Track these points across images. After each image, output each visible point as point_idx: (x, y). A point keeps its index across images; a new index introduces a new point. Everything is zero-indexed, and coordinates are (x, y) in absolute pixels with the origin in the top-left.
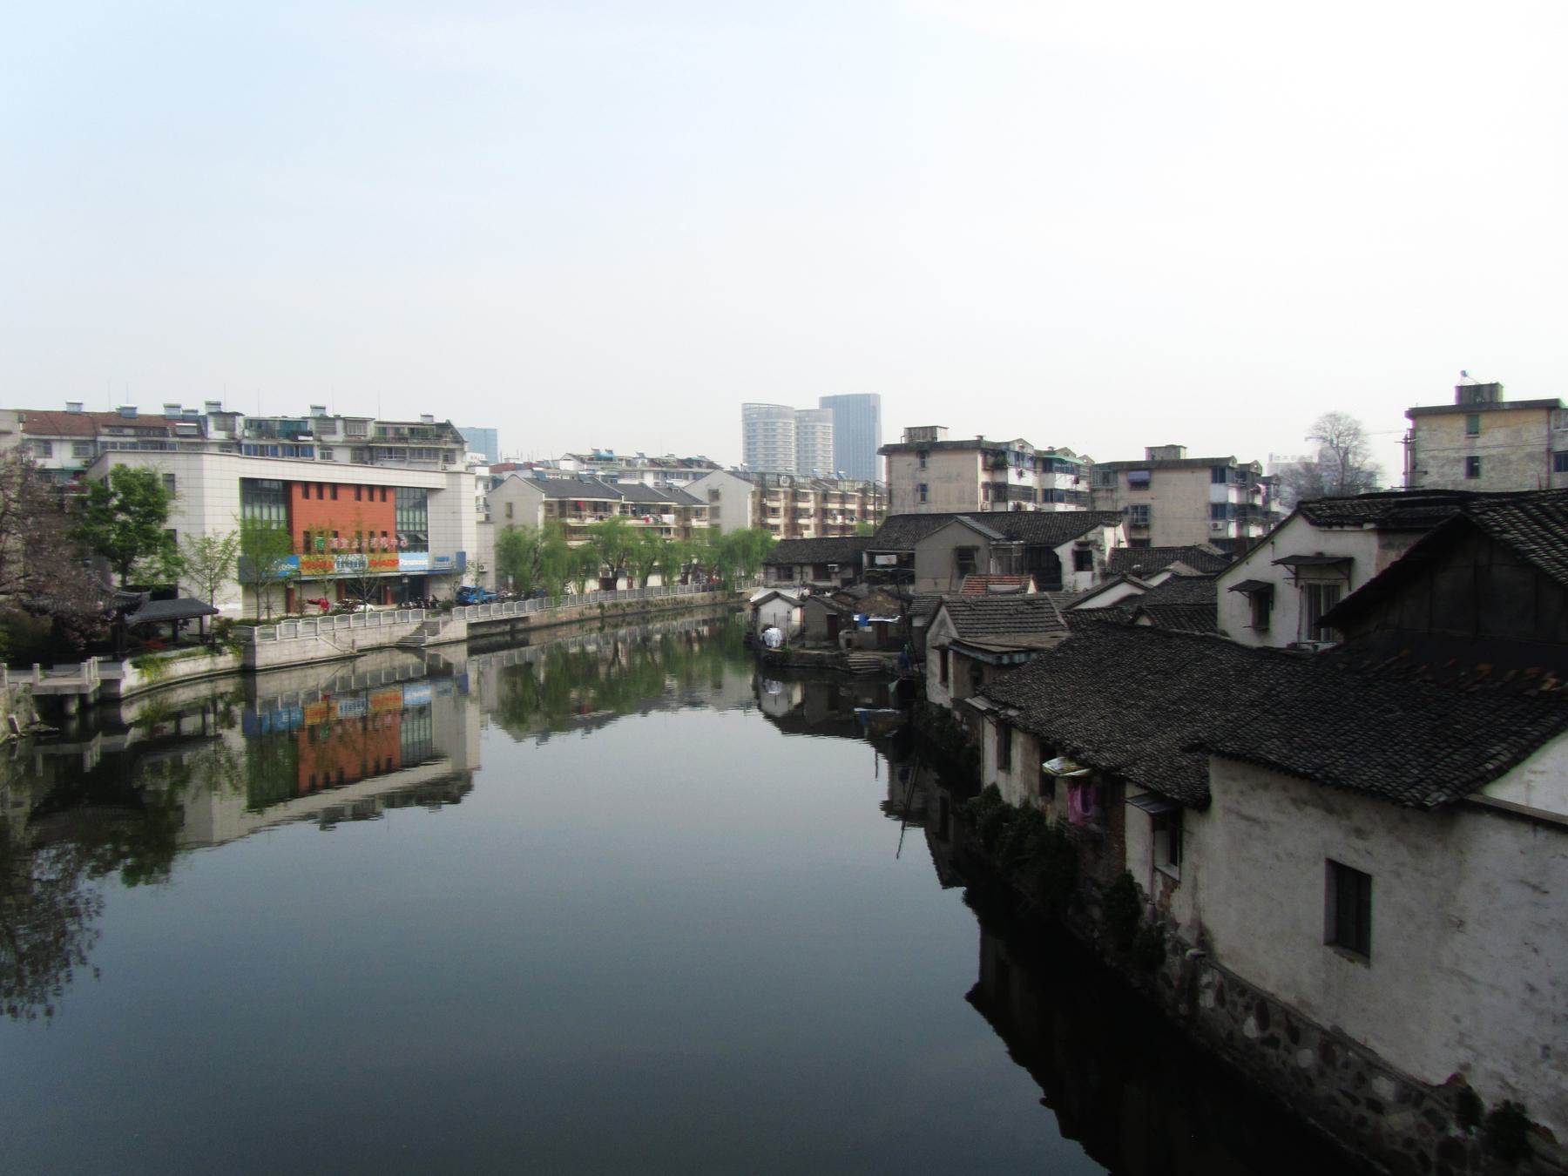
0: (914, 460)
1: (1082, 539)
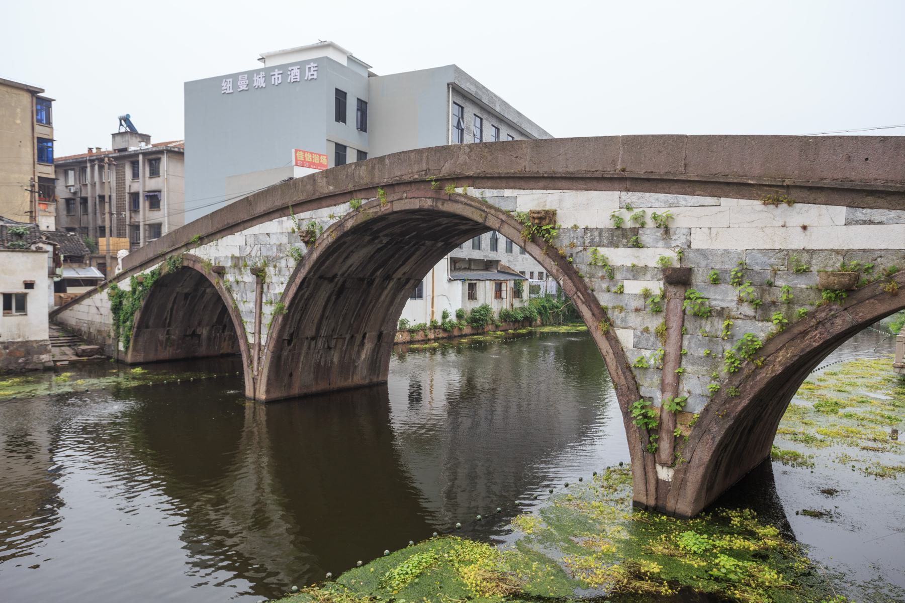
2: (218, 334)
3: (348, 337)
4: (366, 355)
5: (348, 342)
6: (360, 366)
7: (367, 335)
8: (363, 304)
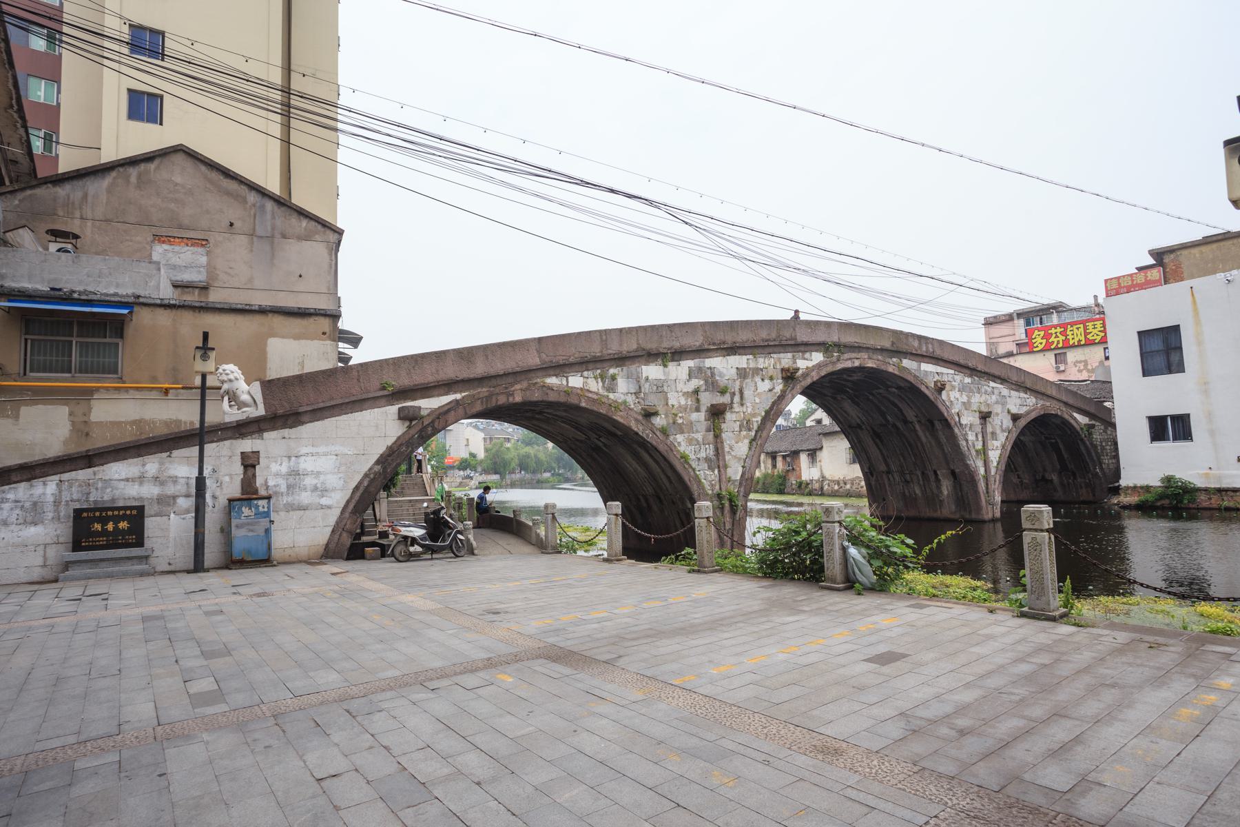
2: (1070, 481)
3: (919, 473)
4: (948, 490)
5: (922, 477)
6: (946, 500)
7: (938, 472)
8: (910, 445)
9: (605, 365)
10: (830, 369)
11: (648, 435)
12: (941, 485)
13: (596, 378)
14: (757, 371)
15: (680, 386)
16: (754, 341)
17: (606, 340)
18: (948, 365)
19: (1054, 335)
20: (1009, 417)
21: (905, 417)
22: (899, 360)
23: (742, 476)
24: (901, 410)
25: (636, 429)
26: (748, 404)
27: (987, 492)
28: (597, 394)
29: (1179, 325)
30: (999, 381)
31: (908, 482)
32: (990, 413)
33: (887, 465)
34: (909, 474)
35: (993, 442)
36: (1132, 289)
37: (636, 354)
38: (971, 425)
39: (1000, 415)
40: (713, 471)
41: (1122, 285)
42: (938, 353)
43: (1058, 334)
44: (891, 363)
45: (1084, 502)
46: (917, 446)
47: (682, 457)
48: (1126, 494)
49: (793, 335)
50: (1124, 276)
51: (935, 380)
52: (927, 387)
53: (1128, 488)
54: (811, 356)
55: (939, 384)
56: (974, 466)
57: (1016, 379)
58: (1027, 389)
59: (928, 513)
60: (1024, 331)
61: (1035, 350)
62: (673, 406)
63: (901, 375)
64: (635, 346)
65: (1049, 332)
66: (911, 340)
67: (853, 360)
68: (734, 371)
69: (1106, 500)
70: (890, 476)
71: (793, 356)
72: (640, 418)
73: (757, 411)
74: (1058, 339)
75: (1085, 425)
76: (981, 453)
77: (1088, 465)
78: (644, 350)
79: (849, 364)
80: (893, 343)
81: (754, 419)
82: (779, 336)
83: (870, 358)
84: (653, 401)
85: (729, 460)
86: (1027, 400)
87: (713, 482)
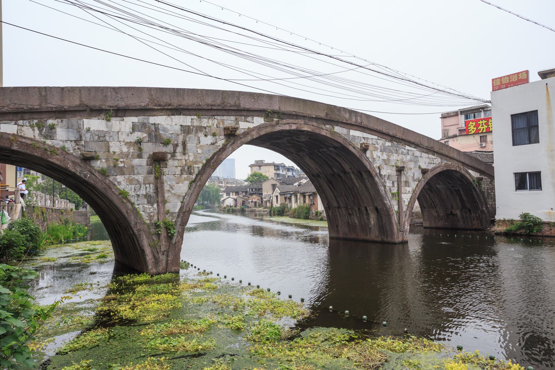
0: (258, 168)
1: (299, 182)
2: (468, 215)
3: (357, 209)
6: (373, 228)
7: (368, 209)
8: (350, 189)
9: (43, 116)
10: (269, 130)
11: (85, 176)
12: (370, 217)
13: (32, 127)
14: (200, 129)
15: (123, 137)
16: (200, 105)
17: (46, 96)
18: (372, 132)
19: (481, 125)
20: (420, 171)
21: (344, 169)
22: (331, 127)
23: (182, 208)
24: (340, 164)
25: (73, 170)
26: (191, 154)
27: (399, 223)
28: (31, 139)
29: (537, 111)
30: (414, 146)
31: (351, 214)
32: (403, 167)
33: (338, 203)
34: (351, 209)
35: (406, 188)
36: (509, 86)
37: (76, 109)
38: (389, 175)
39: (413, 169)
40: (152, 205)
41: (503, 83)
42: (365, 123)
43: (483, 124)
44: (324, 128)
45: (475, 230)
46: (354, 190)
47: (120, 194)
48: (499, 225)
49: (237, 103)
50: (504, 77)
51: (361, 142)
52: (354, 148)
53: (500, 221)
54: (253, 119)
55: (364, 146)
56: (389, 204)
57: (426, 145)
58: (434, 152)
59: (362, 236)
60: (464, 122)
61: (469, 133)
62: (114, 153)
63: (333, 138)
64: (77, 103)
65: (479, 123)
66: (343, 112)
67: (290, 124)
68: (178, 128)
69: (488, 229)
70: (340, 210)
71: (236, 119)
72: (78, 161)
73: (199, 159)
74: (483, 127)
75: (476, 178)
76: (396, 196)
77: (478, 205)
78: (87, 106)
79: (287, 127)
80: (327, 114)
81: (195, 166)
82: (224, 103)
83: (305, 124)
84: (94, 147)
85: (169, 196)
86: (434, 160)
87: (152, 214)
